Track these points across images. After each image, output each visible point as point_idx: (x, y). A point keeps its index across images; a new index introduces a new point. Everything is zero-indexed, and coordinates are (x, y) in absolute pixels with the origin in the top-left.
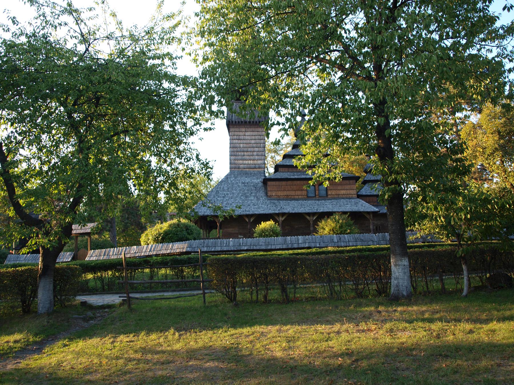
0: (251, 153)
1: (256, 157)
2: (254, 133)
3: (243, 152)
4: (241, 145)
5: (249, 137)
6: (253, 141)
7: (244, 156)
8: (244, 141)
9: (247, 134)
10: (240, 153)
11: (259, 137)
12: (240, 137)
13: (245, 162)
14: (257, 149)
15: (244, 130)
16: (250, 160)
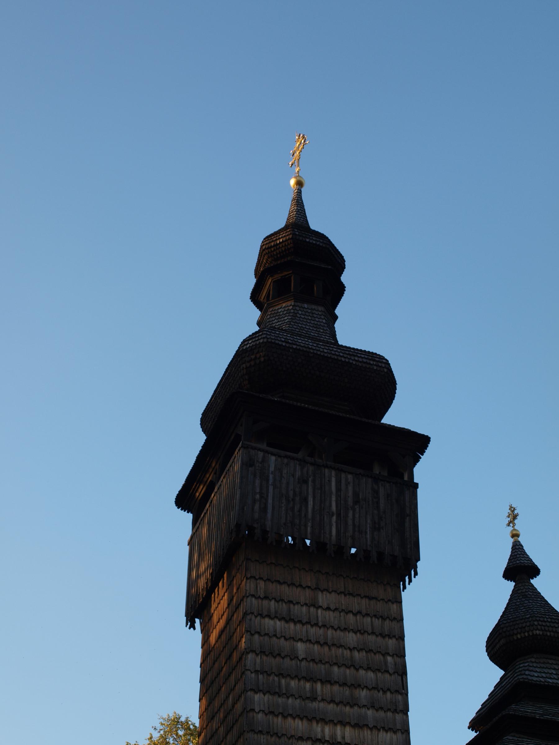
0: (347, 691)
1: (370, 713)
2: (356, 603)
3: (311, 679)
4: (300, 646)
5: (331, 617)
6: (351, 638)
7: (313, 698)
8: (313, 631)
9: (323, 599)
10: (293, 683)
11: (377, 622)
12: (296, 609)
13: (317, 729)
14: (371, 674)
15: (308, 579)
16: (343, 724)
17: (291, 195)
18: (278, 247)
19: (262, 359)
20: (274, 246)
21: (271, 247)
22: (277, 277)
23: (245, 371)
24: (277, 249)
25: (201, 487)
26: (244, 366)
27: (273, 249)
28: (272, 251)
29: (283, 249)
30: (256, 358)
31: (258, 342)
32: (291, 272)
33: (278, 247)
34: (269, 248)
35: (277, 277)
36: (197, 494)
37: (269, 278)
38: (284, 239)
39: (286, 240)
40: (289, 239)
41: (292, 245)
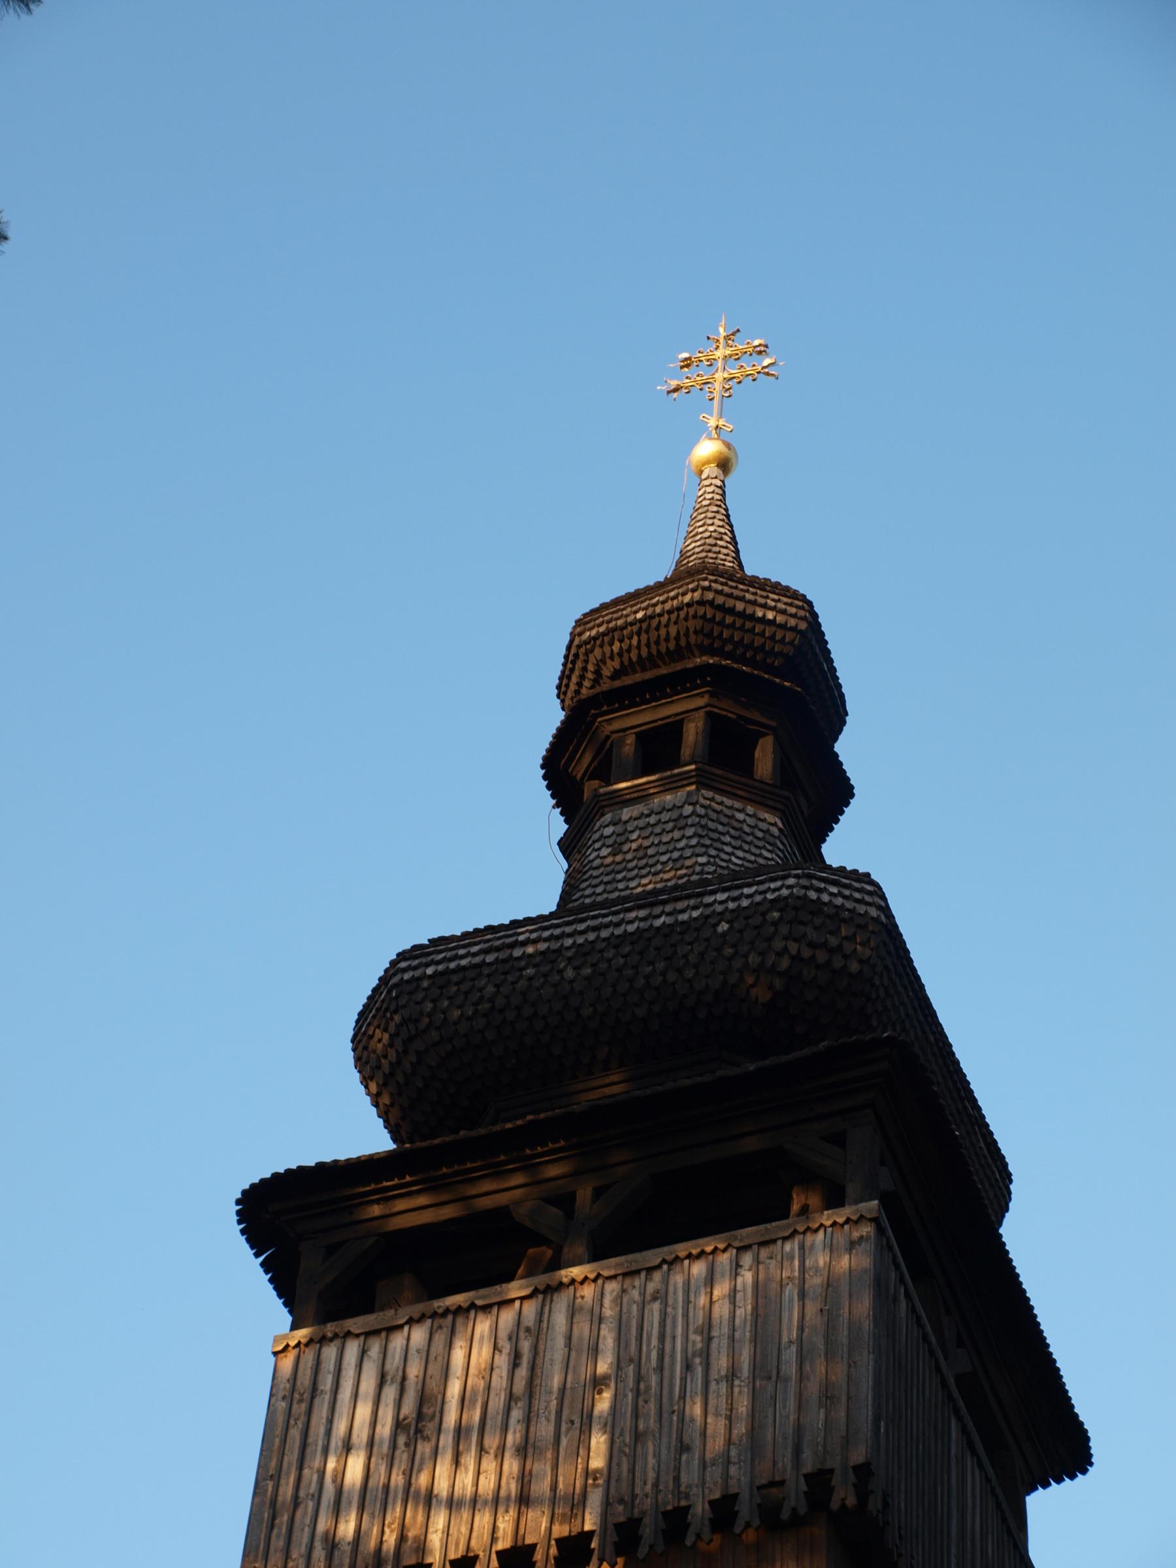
17: (710, 492)
18: (748, 625)
19: (854, 967)
20: (742, 615)
21: (732, 611)
22: (729, 709)
23: (785, 963)
24: (742, 628)
25: (422, 1200)
26: (793, 947)
27: (729, 620)
28: (721, 623)
29: (758, 642)
30: (832, 951)
31: (862, 909)
32: (773, 724)
33: (748, 625)
34: (721, 608)
35: (729, 709)
36: (376, 1210)
37: (701, 695)
38: (780, 619)
39: (783, 626)
40: (794, 629)
41: (788, 650)
